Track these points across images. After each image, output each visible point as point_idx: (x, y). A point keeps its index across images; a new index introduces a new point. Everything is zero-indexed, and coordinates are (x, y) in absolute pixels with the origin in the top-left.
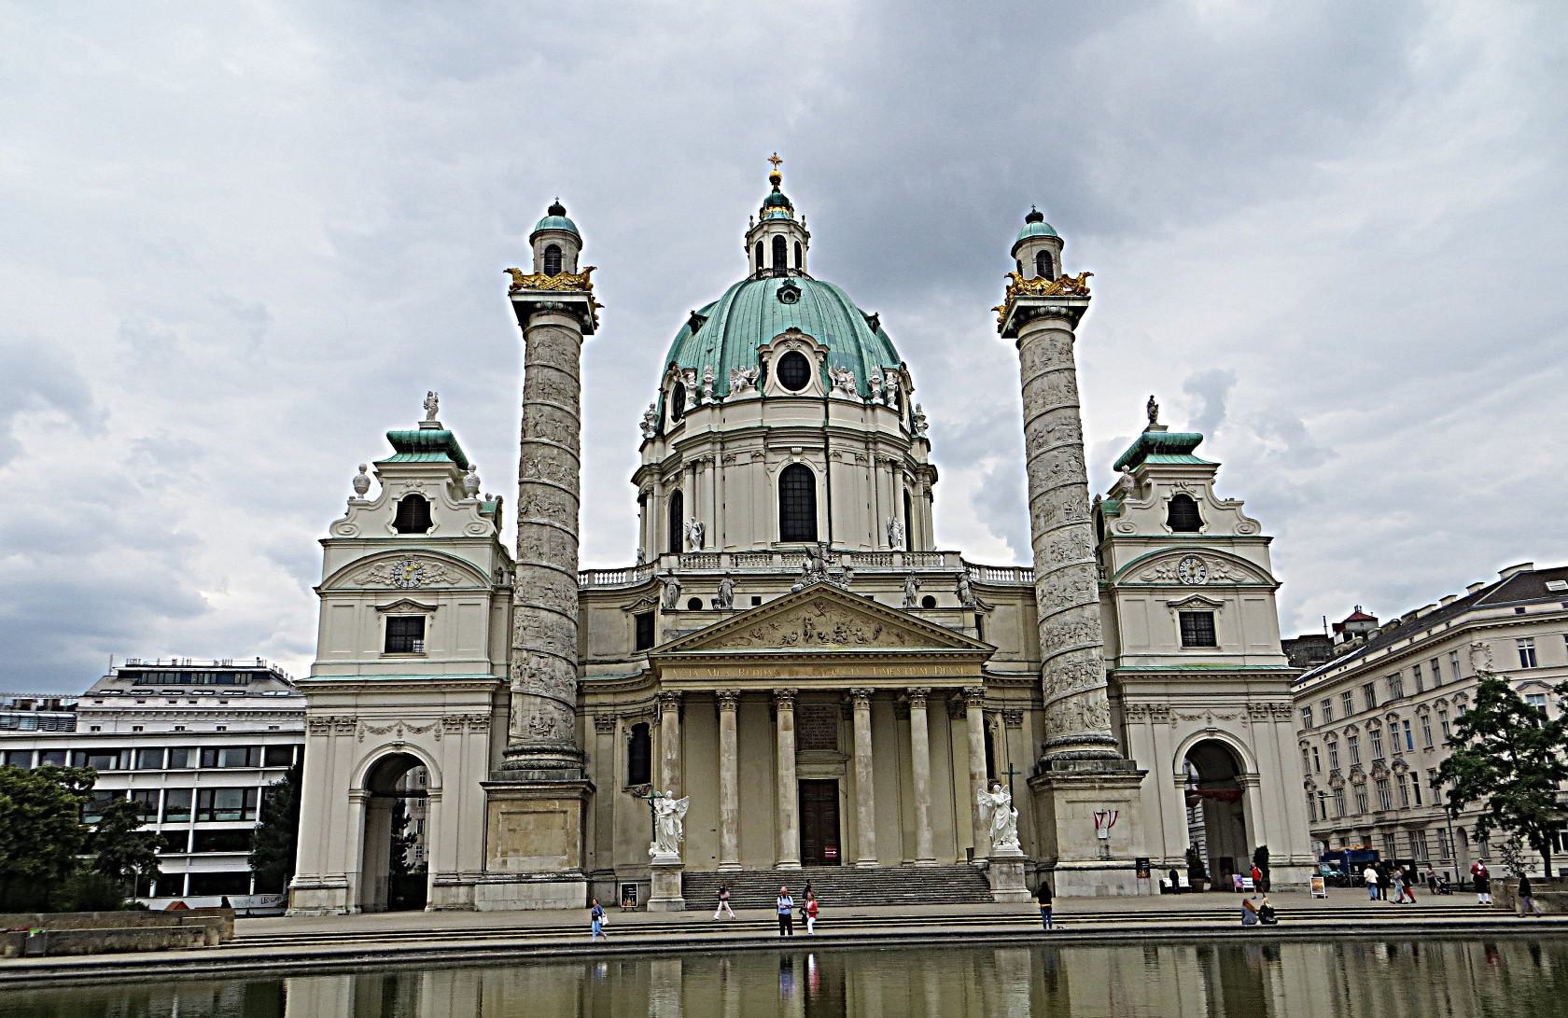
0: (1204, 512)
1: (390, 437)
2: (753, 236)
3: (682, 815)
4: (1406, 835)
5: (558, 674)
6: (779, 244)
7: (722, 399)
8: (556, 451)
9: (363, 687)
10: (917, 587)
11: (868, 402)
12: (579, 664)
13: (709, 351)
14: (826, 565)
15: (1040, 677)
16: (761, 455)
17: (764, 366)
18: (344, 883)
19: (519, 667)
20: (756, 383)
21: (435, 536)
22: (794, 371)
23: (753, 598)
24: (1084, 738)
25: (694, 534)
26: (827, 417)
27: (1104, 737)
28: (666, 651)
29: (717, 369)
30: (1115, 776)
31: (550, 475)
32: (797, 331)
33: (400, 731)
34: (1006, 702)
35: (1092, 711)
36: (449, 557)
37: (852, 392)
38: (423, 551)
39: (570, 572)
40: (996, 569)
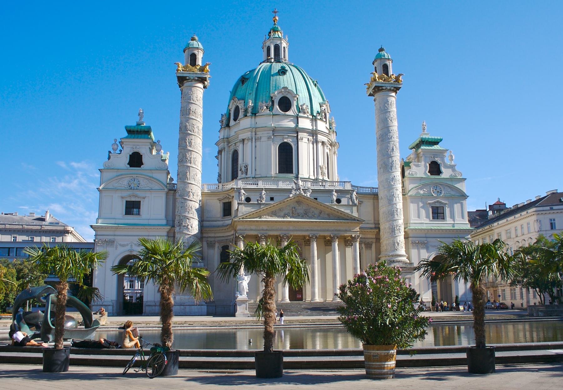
0: (442, 169)
1: (126, 127)
2: (265, 43)
3: (248, 282)
4: (509, 289)
5: (194, 226)
6: (277, 48)
7: (255, 114)
8: (194, 137)
9: (117, 228)
12: (201, 221)
13: (250, 94)
14: (301, 186)
15: (379, 230)
16: (271, 138)
17: (273, 102)
18: (112, 304)
19: (179, 222)
20: (269, 108)
21: (144, 168)
22: (285, 104)
23: (271, 198)
25: (243, 169)
26: (298, 123)
28: (240, 219)
29: (254, 101)
31: (190, 146)
32: (285, 88)
33: (131, 246)
34: (366, 240)
36: (150, 177)
38: (140, 174)
39: (198, 185)
40: (363, 188)
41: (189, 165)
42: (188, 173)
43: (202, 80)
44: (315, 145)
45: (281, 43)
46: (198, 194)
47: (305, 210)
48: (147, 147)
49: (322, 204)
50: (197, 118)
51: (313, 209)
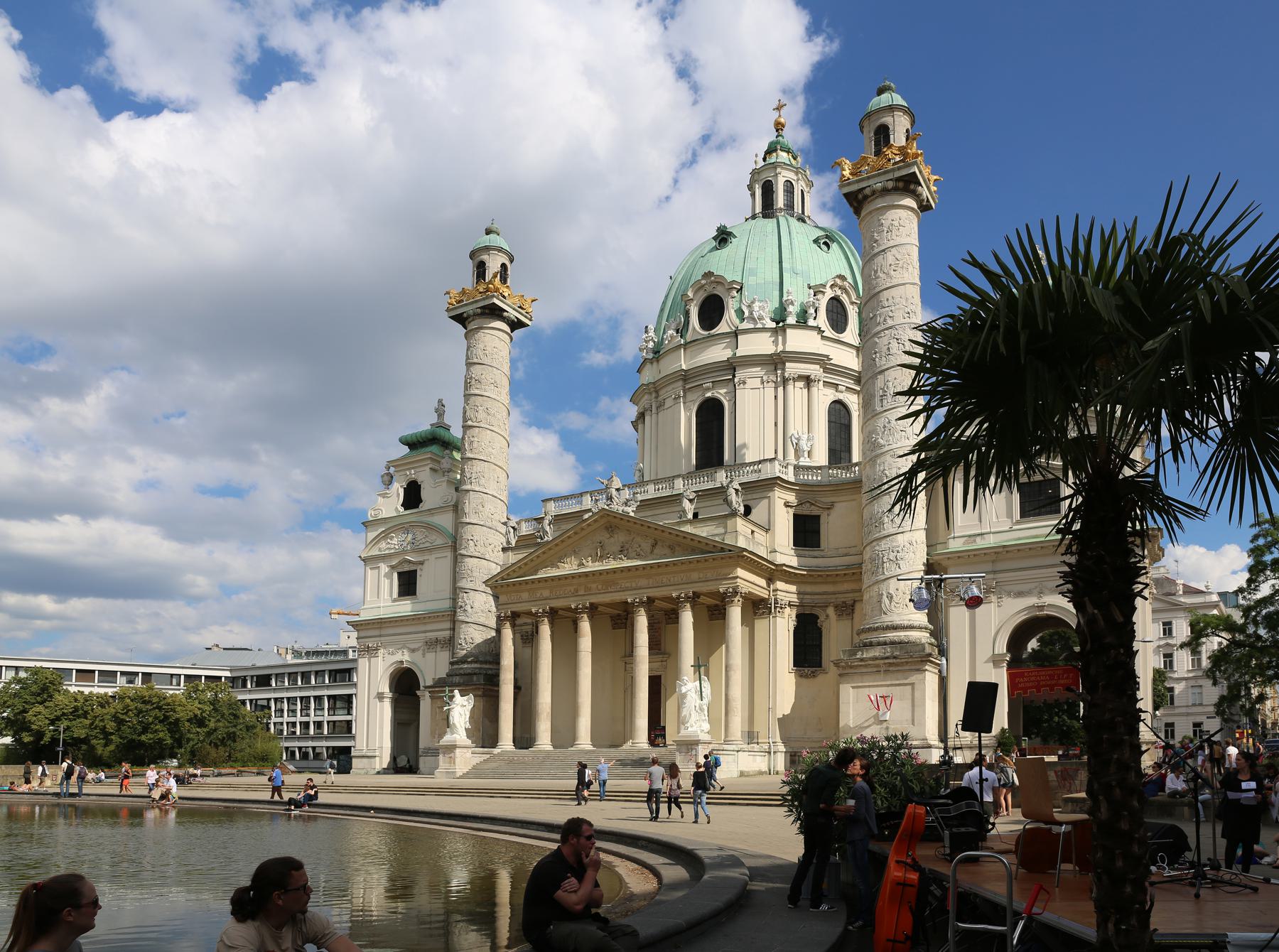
6: (768, 190)
8: (477, 429)
10: (691, 501)
11: (781, 324)
14: (614, 493)
16: (679, 397)
17: (687, 314)
20: (682, 330)
22: (712, 310)
24: (876, 625)
27: (898, 623)
28: (497, 581)
30: (898, 660)
32: (708, 275)
35: (892, 597)
36: (429, 524)
37: (761, 318)
39: (487, 524)
41: (468, 487)
42: (467, 503)
43: (495, 312)
44: (780, 390)
45: (776, 175)
46: (490, 541)
47: (623, 542)
48: (427, 468)
49: (650, 525)
50: (485, 391)
51: (638, 539)
